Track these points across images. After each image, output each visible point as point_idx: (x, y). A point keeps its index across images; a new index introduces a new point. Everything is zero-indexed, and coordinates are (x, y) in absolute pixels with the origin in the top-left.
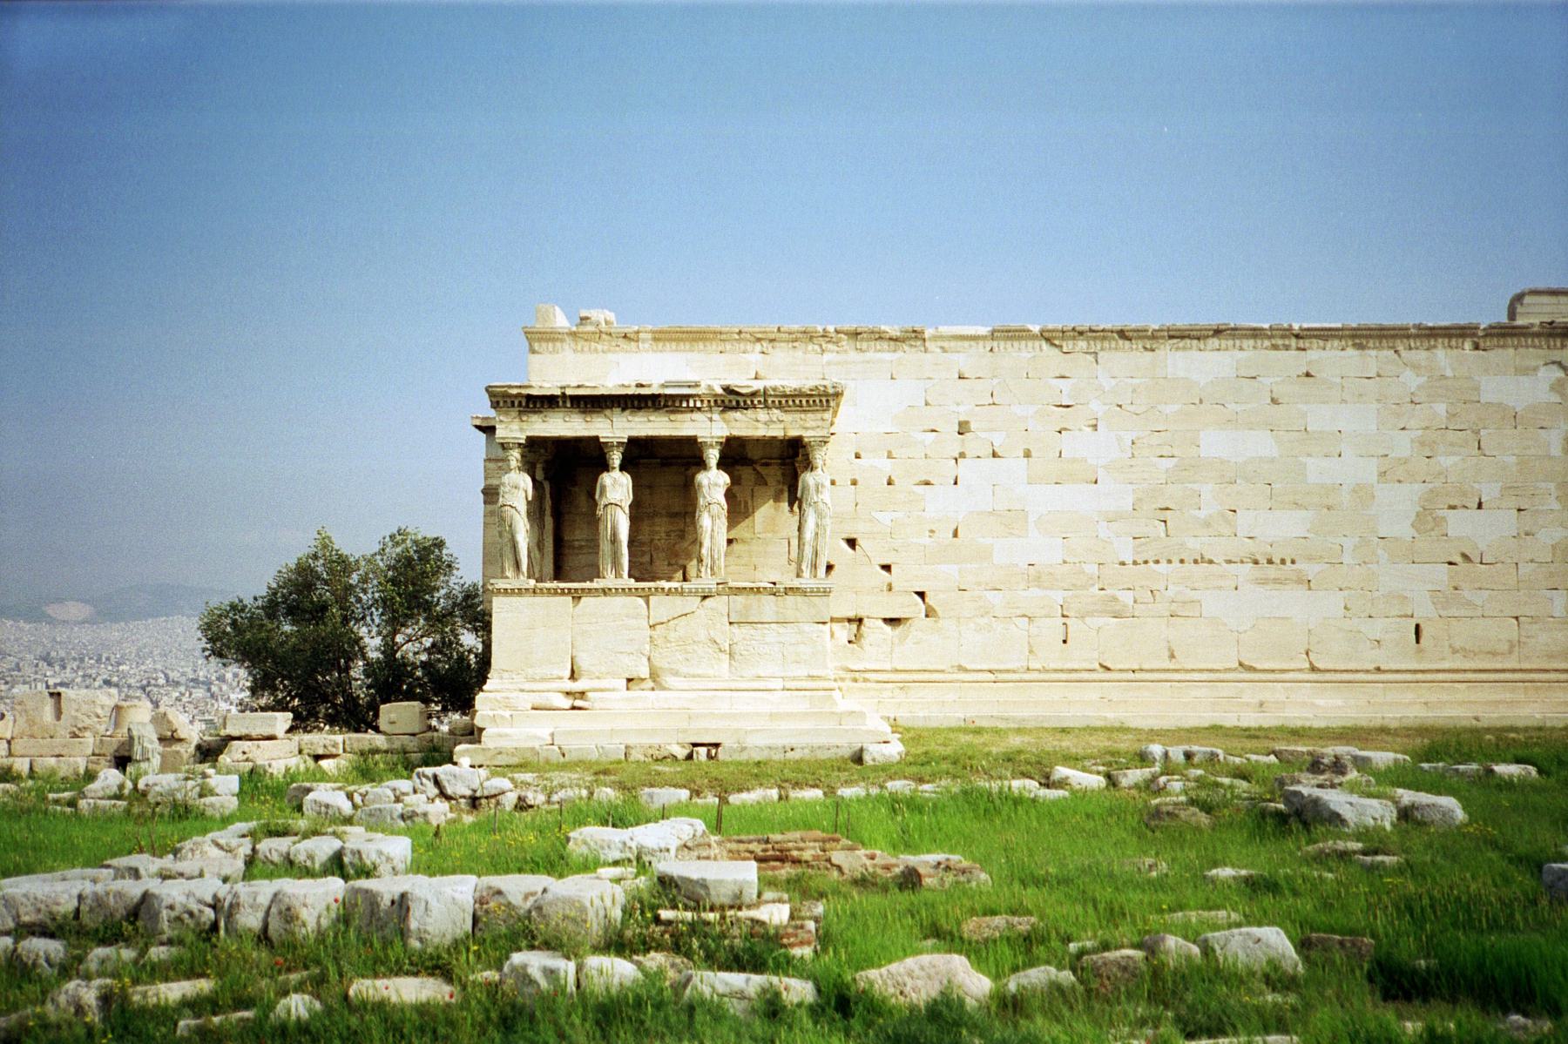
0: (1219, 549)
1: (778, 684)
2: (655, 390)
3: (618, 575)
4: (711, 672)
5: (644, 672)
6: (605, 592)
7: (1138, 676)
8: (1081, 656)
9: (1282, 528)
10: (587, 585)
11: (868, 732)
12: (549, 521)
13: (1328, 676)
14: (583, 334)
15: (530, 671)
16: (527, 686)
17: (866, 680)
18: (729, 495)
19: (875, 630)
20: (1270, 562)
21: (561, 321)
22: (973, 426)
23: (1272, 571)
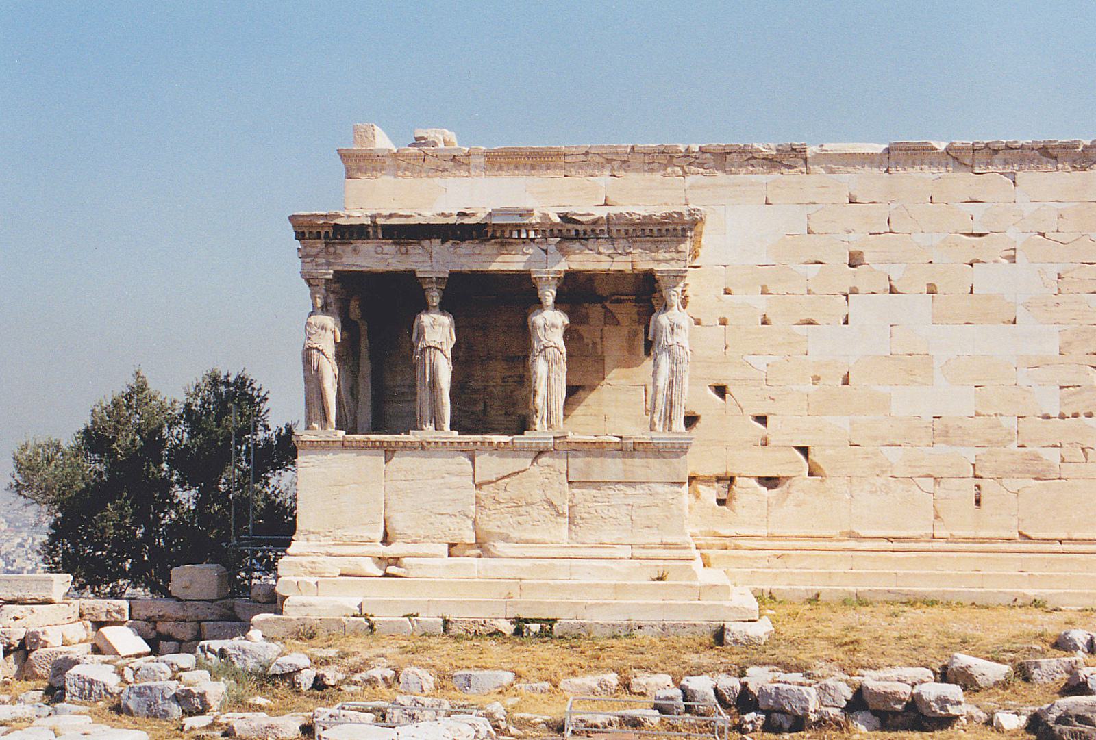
1: (625, 552)
3: (438, 427)
4: (547, 538)
5: (470, 537)
6: (423, 446)
7: (1066, 547)
8: (998, 522)
10: (403, 437)
11: (730, 609)
12: (366, 367)
14: (421, 158)
15: (339, 533)
16: (335, 550)
17: (736, 548)
18: (568, 335)
19: (749, 492)
21: (382, 142)
22: (866, 258)
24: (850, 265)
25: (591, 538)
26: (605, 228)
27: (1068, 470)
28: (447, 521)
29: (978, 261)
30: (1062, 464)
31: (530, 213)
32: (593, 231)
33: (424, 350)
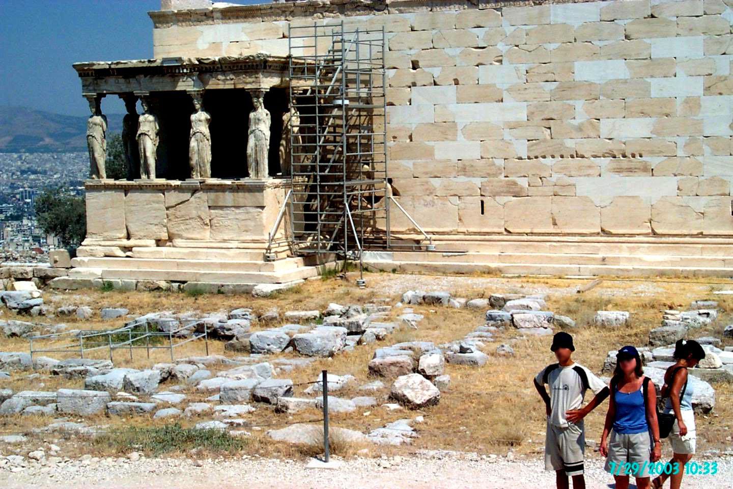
0: (586, 147)
2: (158, 63)
4: (198, 236)
5: (164, 236)
8: (492, 224)
9: (634, 130)
13: (663, 239)
15: (106, 234)
16: (103, 243)
20: (624, 156)
22: (420, 64)
23: (625, 163)
24: (414, 68)
25: (220, 237)
26: (219, 66)
27: (532, 190)
28: (154, 228)
29: (482, 64)
30: (529, 188)
31: (180, 60)
32: (214, 67)
33: (140, 135)
